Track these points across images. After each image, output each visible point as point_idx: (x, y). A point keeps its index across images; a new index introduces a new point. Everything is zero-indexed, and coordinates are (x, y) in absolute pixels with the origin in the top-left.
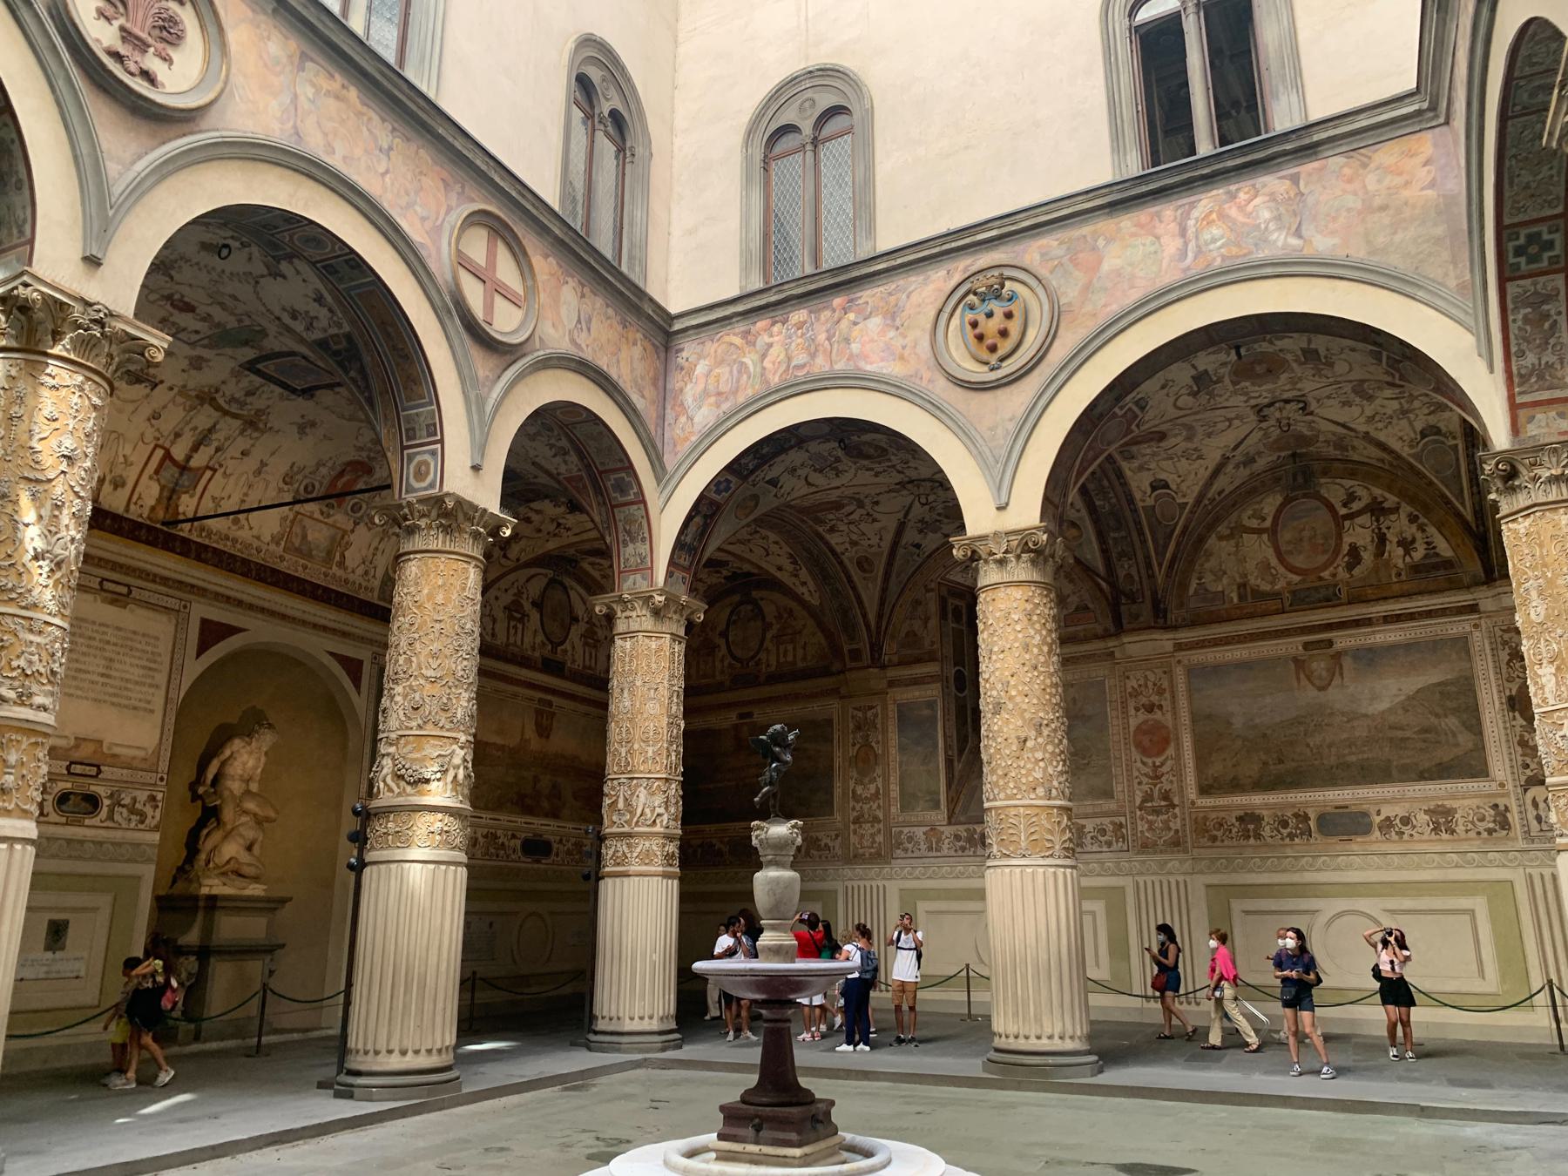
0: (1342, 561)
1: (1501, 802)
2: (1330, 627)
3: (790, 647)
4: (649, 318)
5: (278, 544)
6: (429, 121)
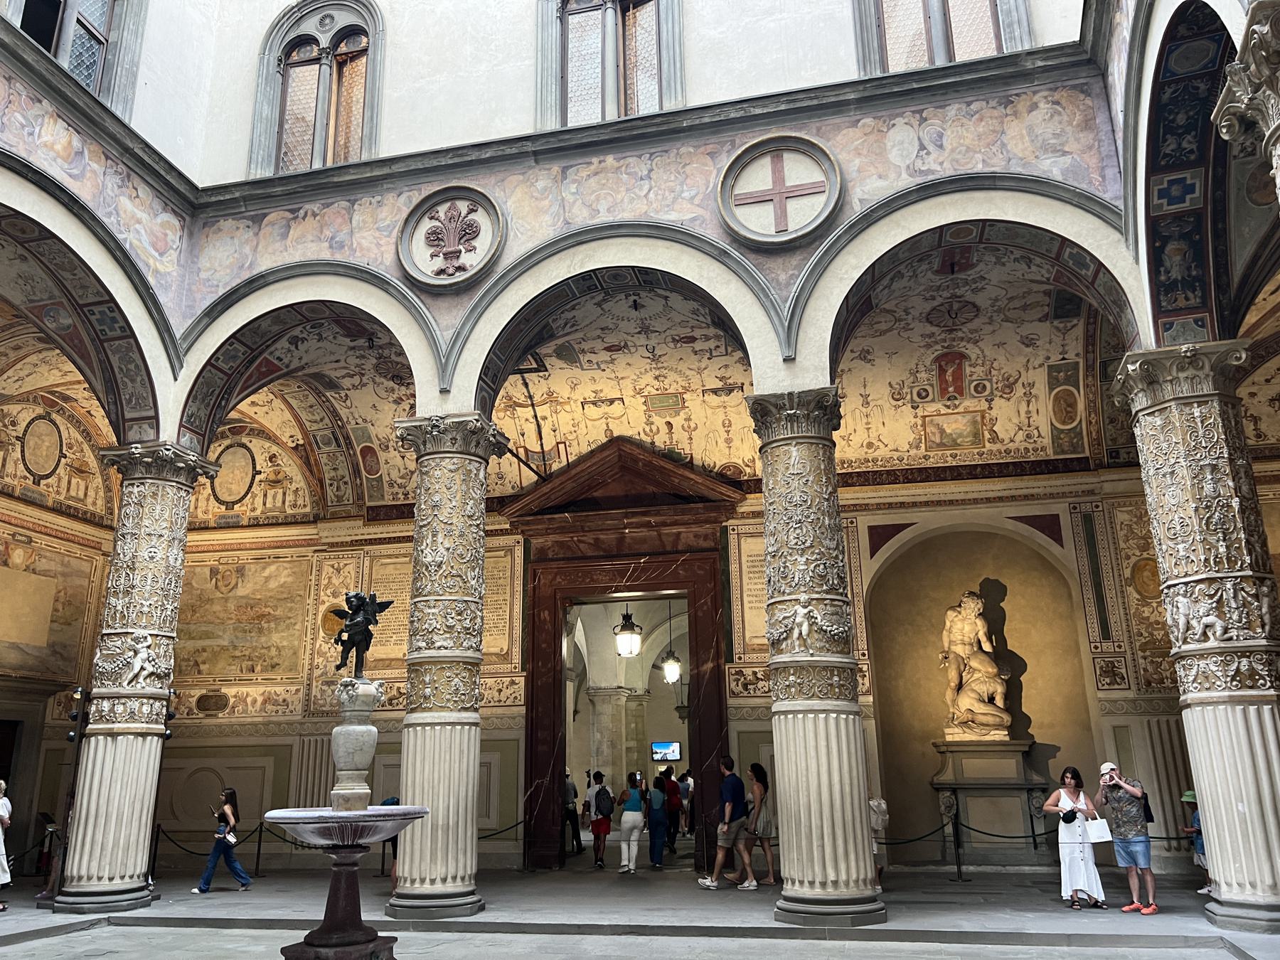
4: (1045, 69)
5: (918, 447)
6: (672, 126)
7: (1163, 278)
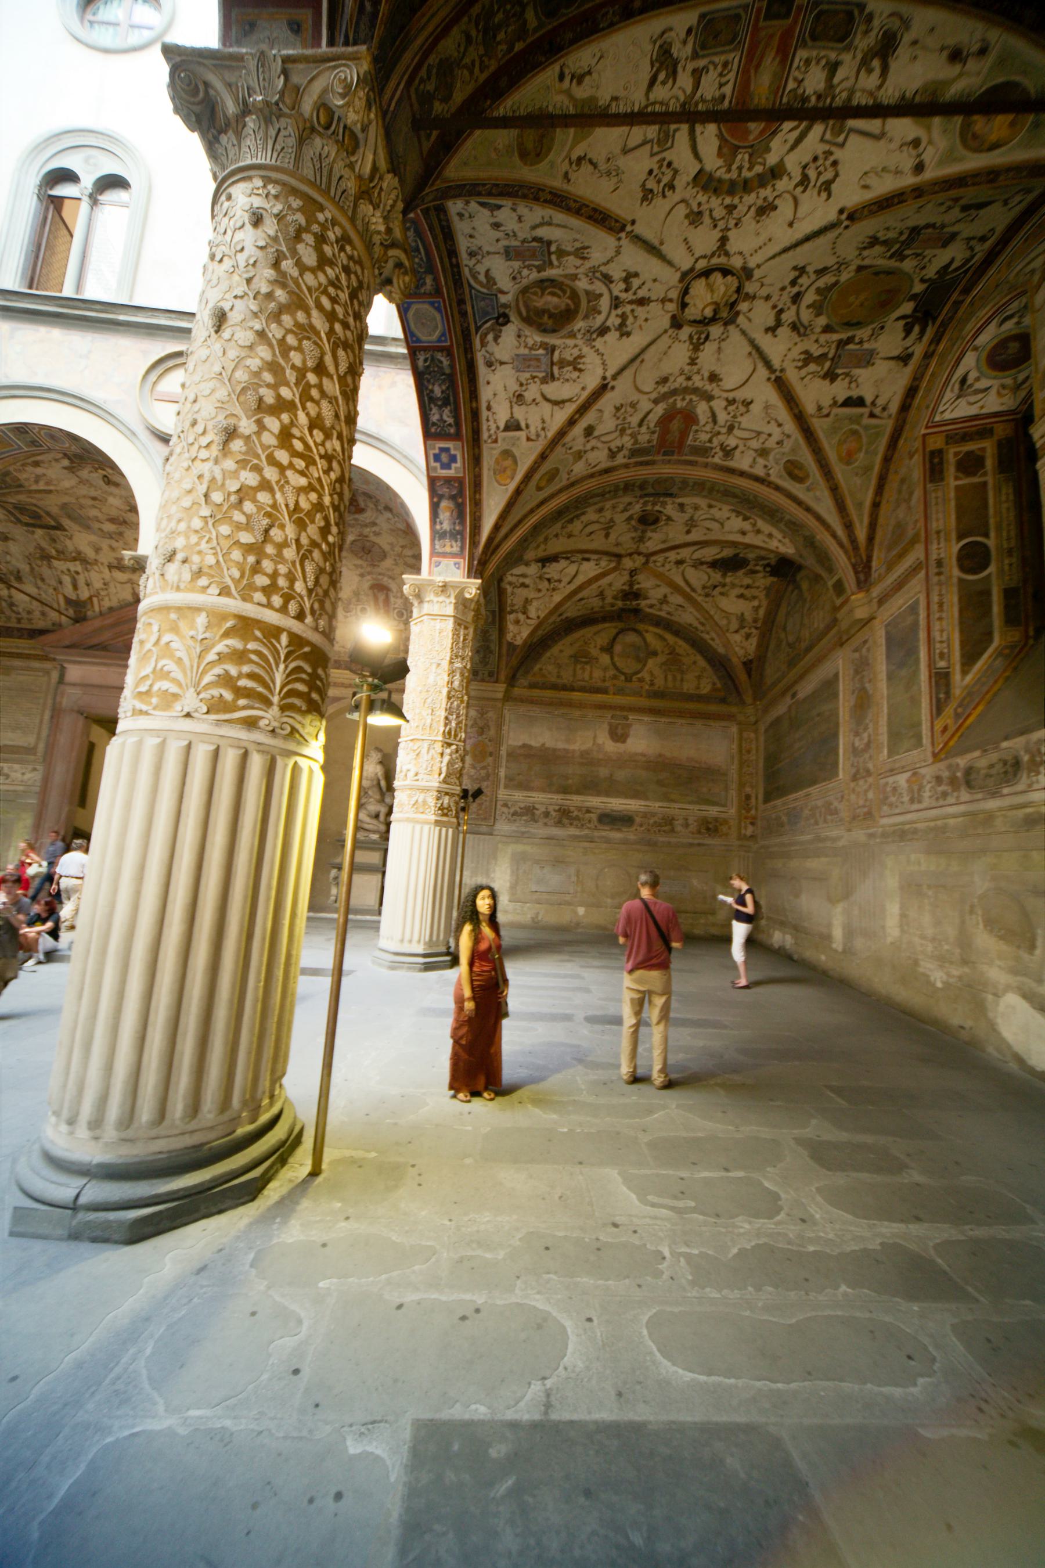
7: (438, 527)
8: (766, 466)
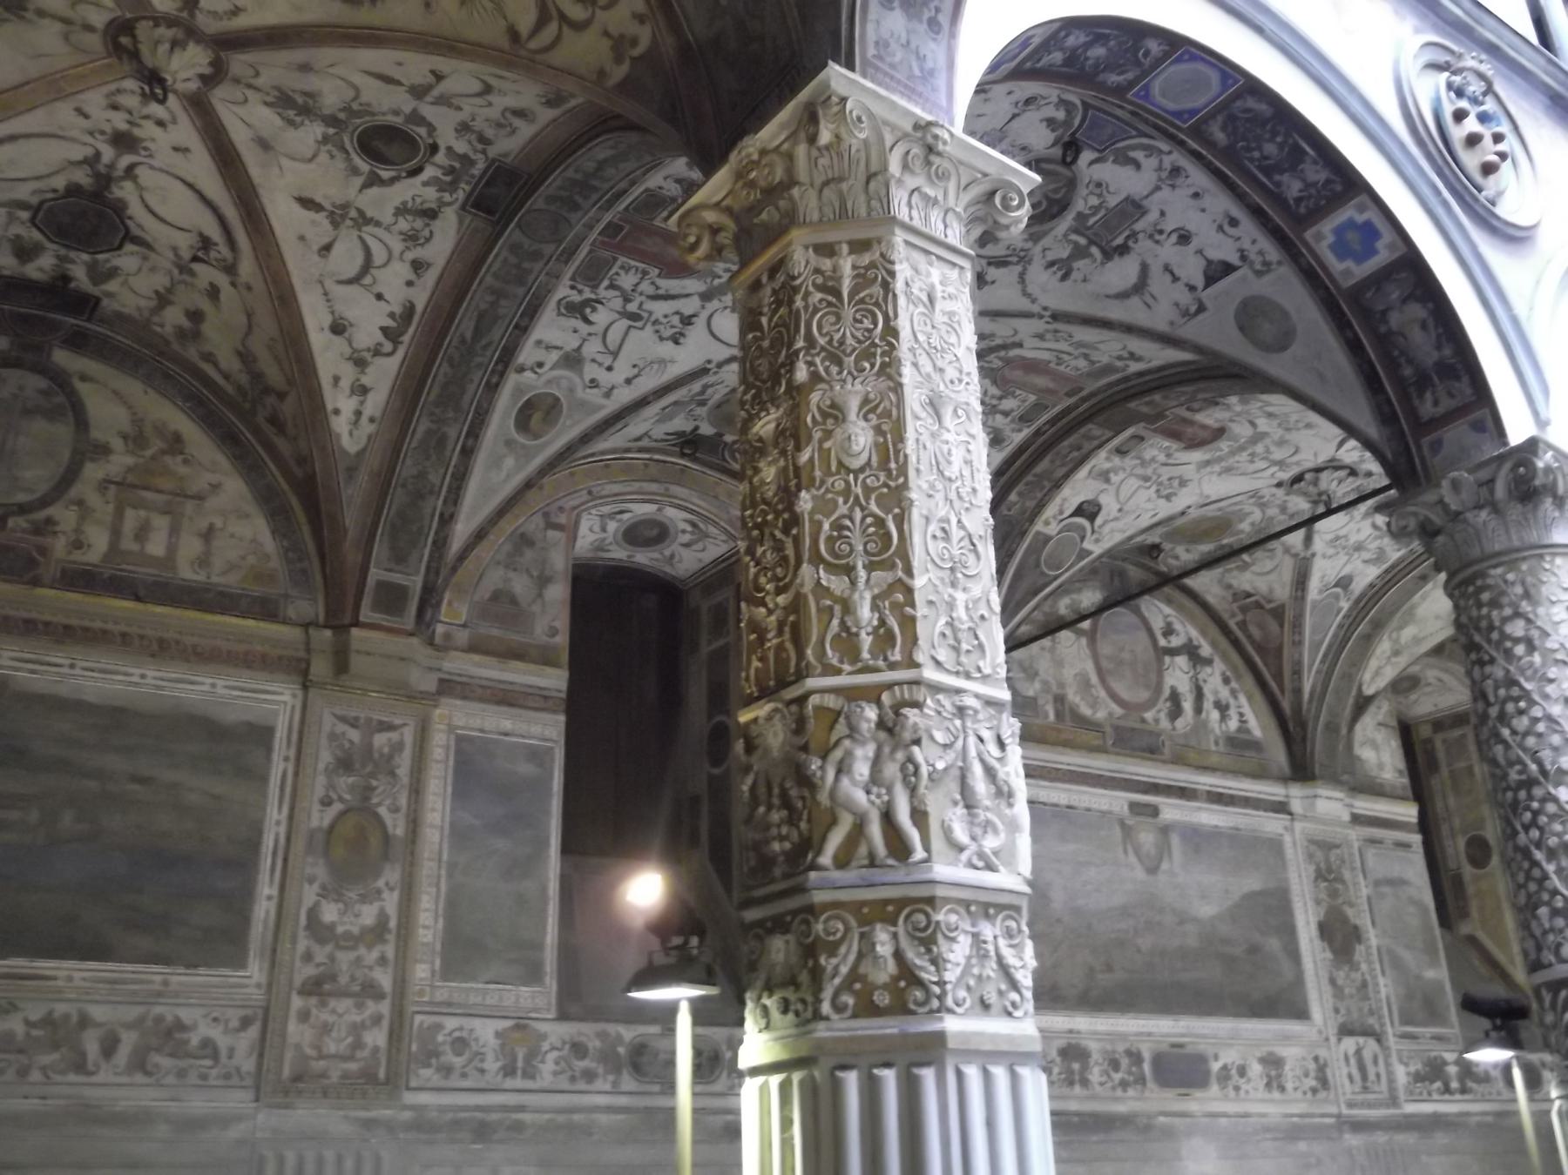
0: (1164, 706)
1: (1323, 1053)
2: (1155, 788)
3: (161, 523)
8: (540, 365)
